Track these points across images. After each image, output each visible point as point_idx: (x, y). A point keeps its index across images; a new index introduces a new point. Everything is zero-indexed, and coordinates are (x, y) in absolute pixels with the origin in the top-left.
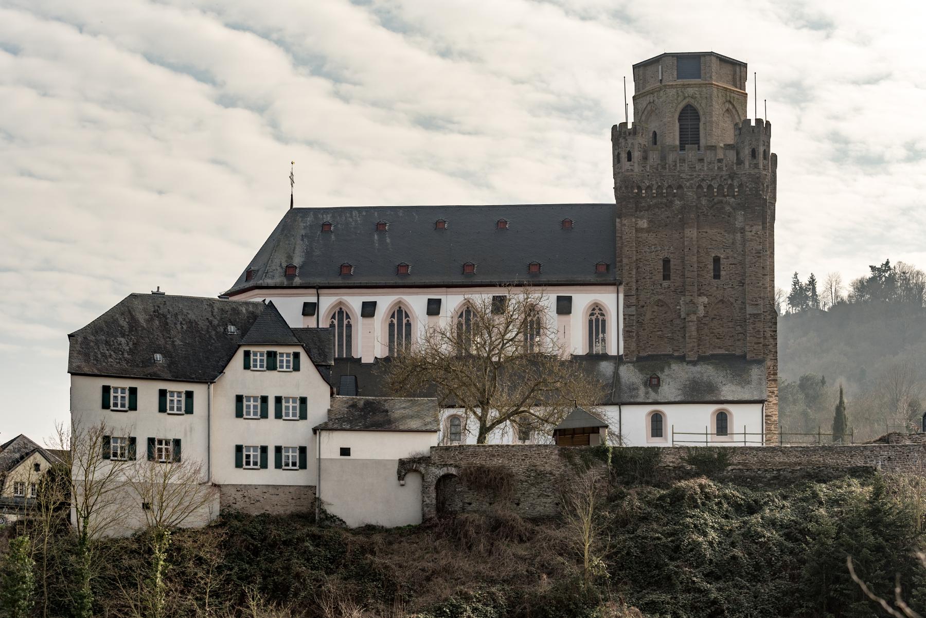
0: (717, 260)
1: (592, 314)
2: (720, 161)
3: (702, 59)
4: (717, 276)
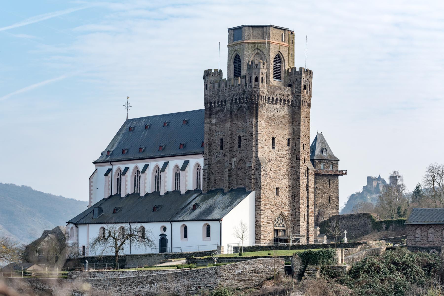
0: (240, 137)
1: (198, 169)
2: (239, 85)
3: (243, 29)
4: (239, 147)
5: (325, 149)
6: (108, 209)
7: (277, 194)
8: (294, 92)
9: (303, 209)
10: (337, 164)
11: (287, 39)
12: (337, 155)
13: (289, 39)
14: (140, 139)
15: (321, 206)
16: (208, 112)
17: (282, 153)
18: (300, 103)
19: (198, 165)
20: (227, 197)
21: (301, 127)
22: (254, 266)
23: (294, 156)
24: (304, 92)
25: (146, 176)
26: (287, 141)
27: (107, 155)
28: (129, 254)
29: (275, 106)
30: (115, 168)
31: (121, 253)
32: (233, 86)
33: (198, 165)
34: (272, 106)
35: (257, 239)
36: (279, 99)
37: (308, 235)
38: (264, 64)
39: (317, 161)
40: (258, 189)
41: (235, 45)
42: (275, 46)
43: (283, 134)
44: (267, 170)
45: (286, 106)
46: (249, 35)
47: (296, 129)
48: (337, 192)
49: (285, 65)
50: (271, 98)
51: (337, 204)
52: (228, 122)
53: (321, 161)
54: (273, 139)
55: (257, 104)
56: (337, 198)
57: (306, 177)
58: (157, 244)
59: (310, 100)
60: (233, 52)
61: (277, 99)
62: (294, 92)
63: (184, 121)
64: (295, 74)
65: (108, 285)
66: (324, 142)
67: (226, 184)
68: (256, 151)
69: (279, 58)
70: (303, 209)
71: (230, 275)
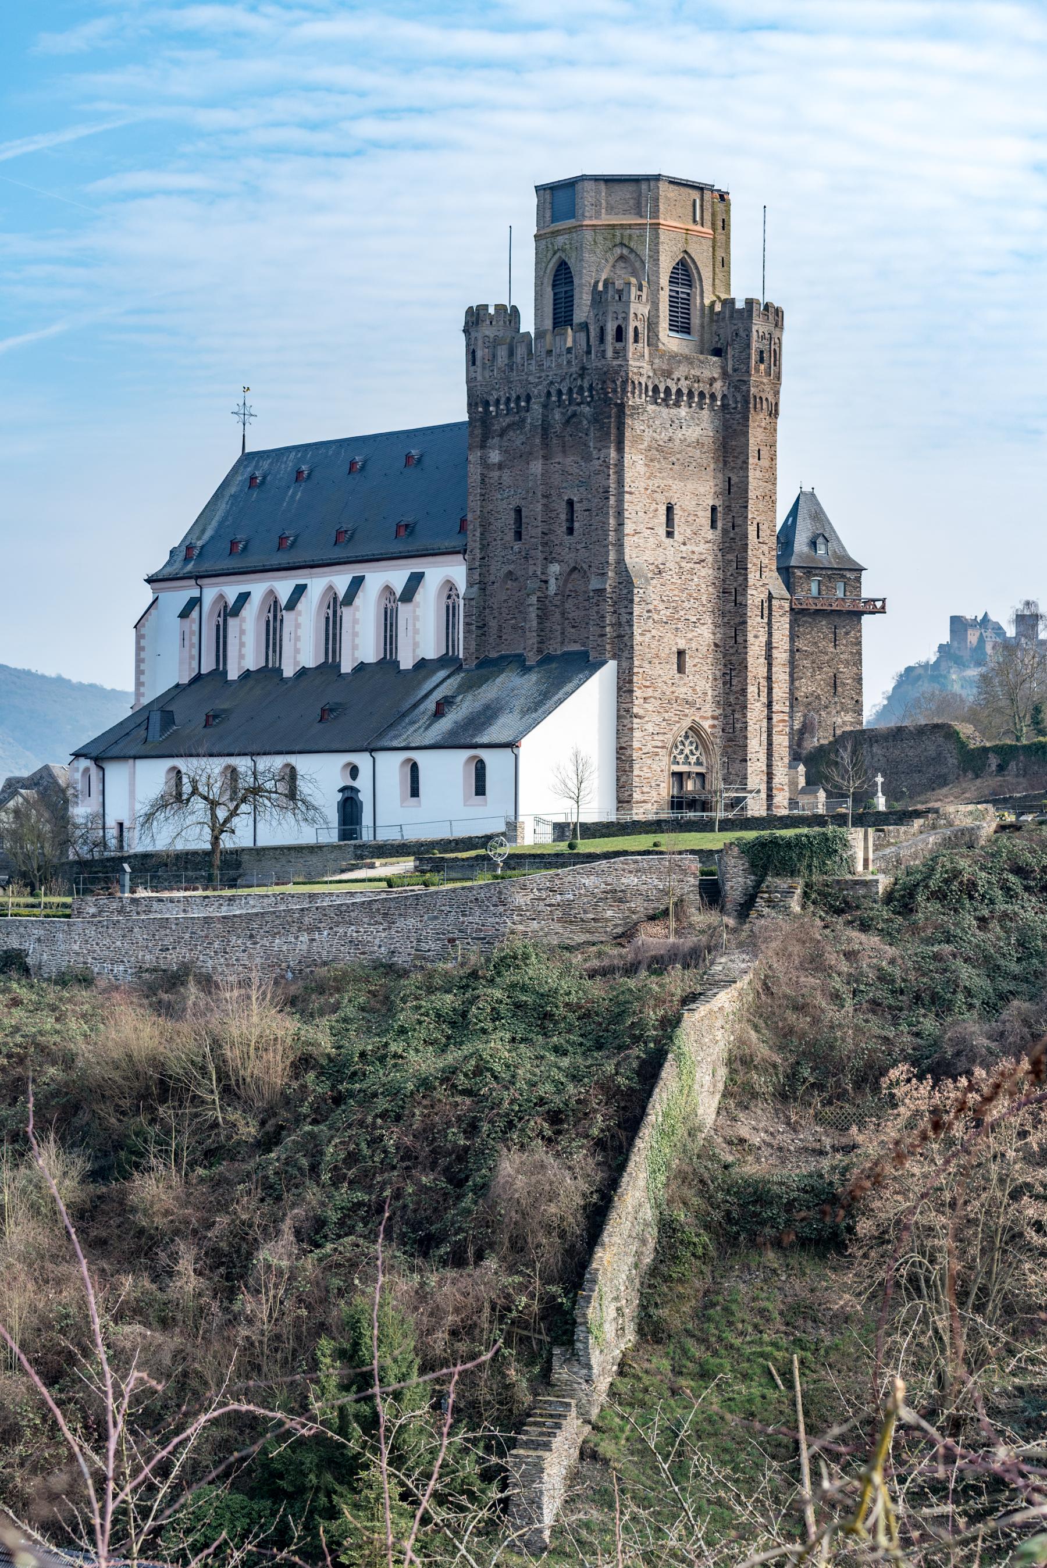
0: (570, 503)
1: (449, 597)
2: (569, 350)
4: (570, 531)
5: (823, 535)
6: (189, 716)
7: (681, 669)
8: (730, 370)
9: (756, 713)
10: (858, 580)
11: (708, 217)
12: (856, 553)
13: (713, 214)
14: (284, 511)
15: (810, 704)
16: (478, 431)
17: (696, 549)
18: (747, 402)
19: (450, 586)
20: (533, 677)
21: (751, 473)
22: (609, 880)
23: (730, 557)
24: (757, 371)
25: (300, 620)
26: (709, 514)
27: (187, 559)
28: (251, 845)
29: (674, 411)
30: (210, 594)
31: (227, 842)
32: (549, 352)
33: (450, 586)
34: (665, 411)
35: (623, 801)
36: (685, 391)
37: (770, 789)
38: (640, 289)
39: (799, 573)
40: (626, 654)
41: (555, 234)
42: (673, 235)
43: (697, 494)
44: (649, 597)
45: (705, 413)
46: (597, 204)
47: (735, 479)
48: (858, 663)
49: (702, 292)
50: (662, 388)
51: (856, 697)
52: (536, 458)
53: (809, 571)
54: (670, 509)
55: (621, 407)
56: (859, 680)
57: (766, 620)
58: (333, 816)
59: (777, 393)
60: (549, 255)
61: (679, 392)
62: (730, 370)
63: (408, 457)
64: (731, 317)
65: (187, 936)
66: (818, 515)
67: (532, 639)
68: (620, 545)
69: (684, 272)
70: (756, 713)
71: (541, 906)
